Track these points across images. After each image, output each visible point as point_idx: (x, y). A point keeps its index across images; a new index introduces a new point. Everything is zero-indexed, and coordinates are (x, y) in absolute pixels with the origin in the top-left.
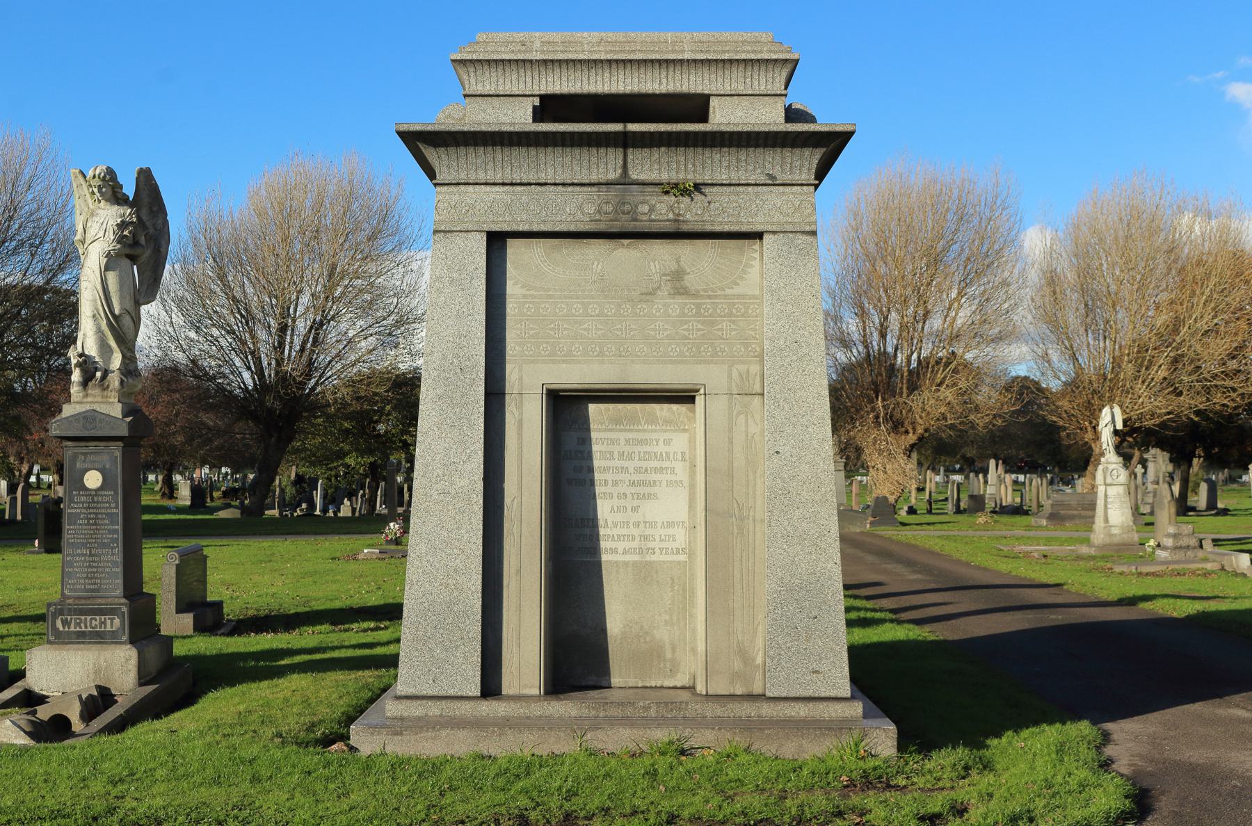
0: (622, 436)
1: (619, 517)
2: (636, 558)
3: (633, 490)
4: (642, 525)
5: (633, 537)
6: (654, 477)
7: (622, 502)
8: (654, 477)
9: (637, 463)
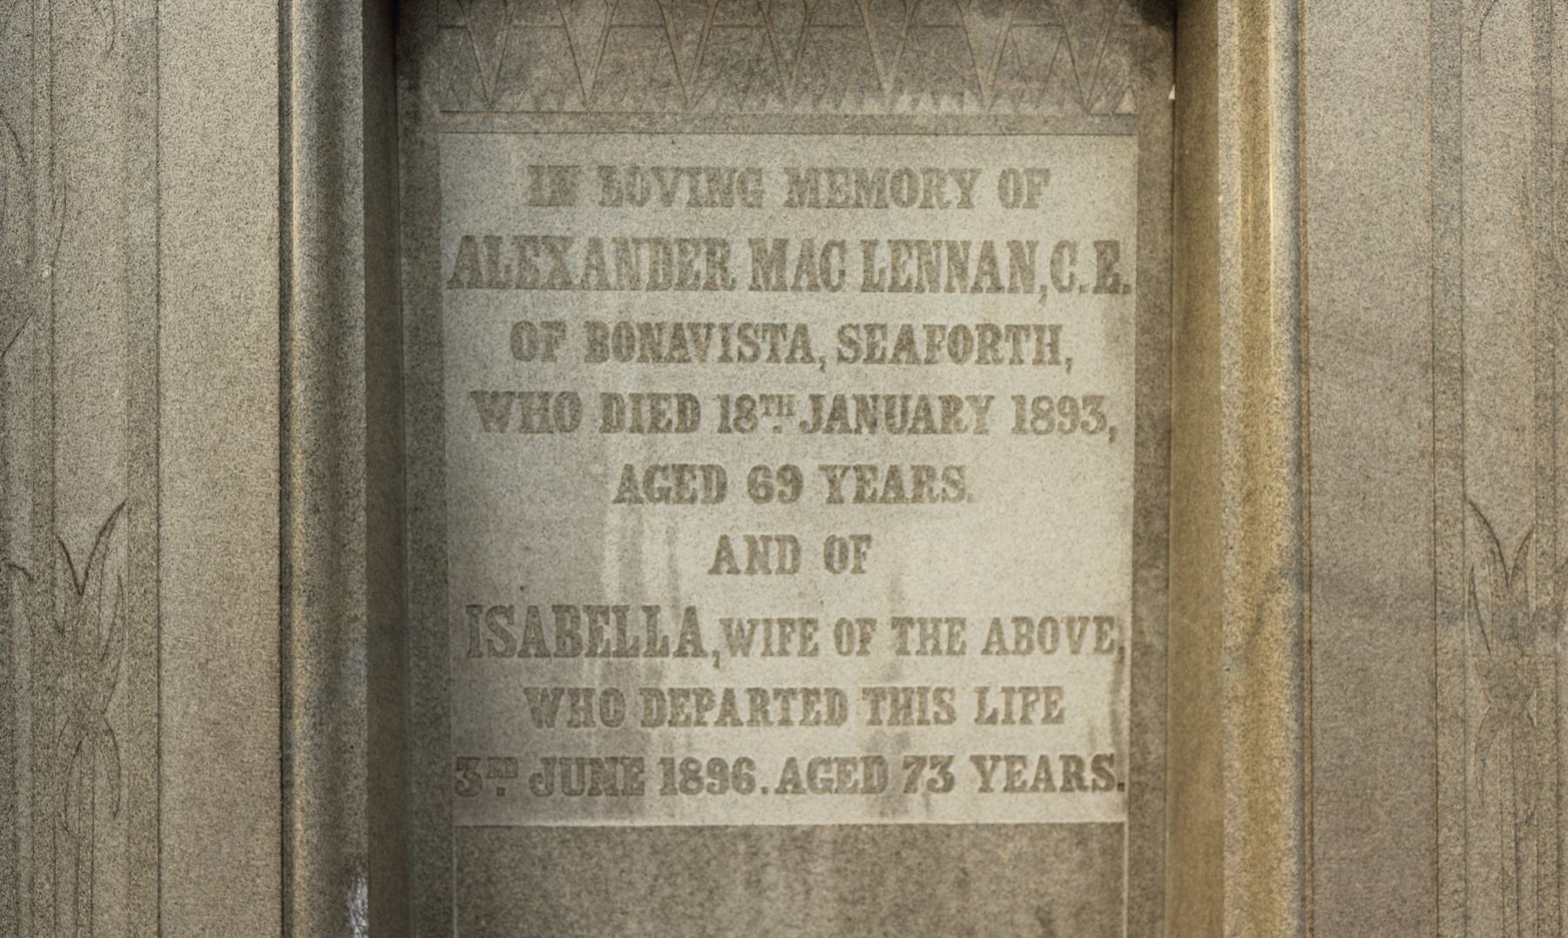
0: (776, 157)
1: (761, 597)
2: (853, 811)
3: (838, 450)
4: (884, 635)
5: (759, 490)
6: (952, 377)
7: (774, 517)
8: (952, 377)
9: (861, 308)
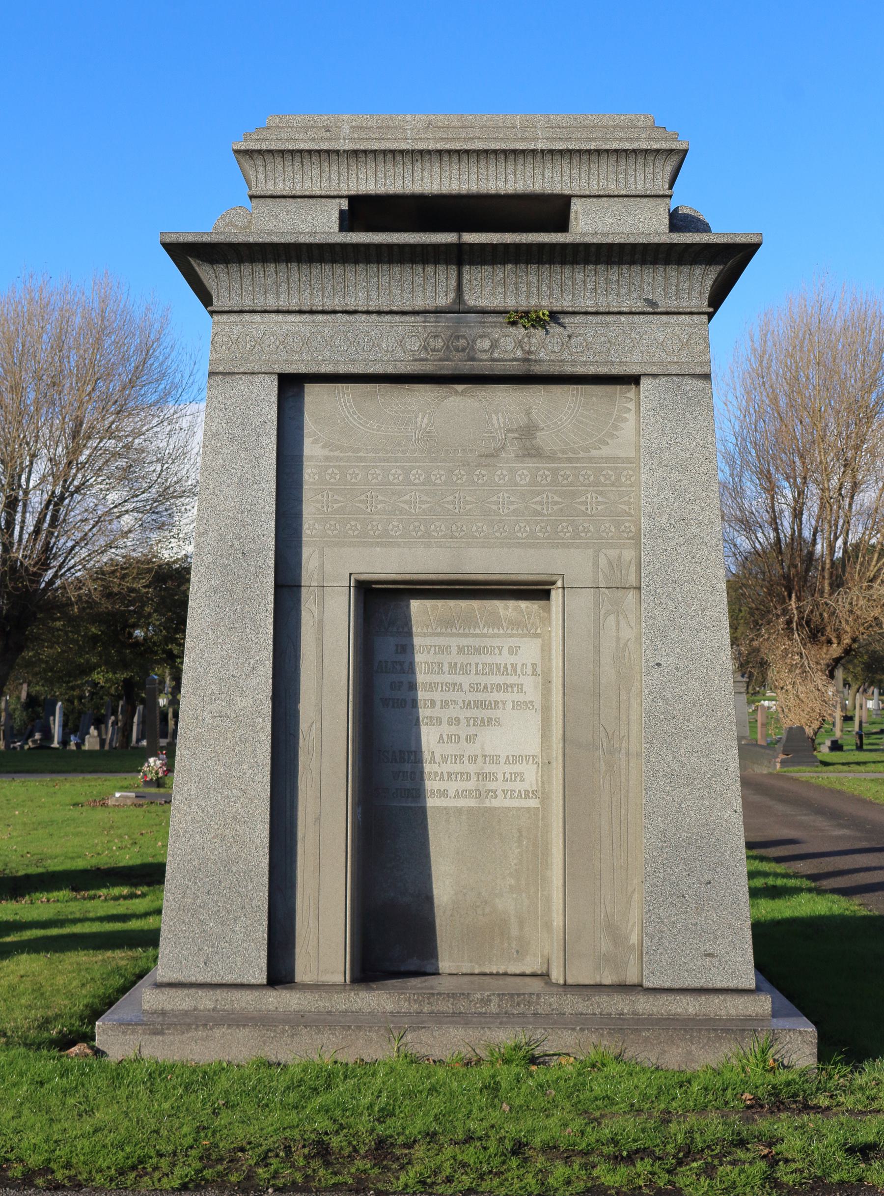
0: (454, 643)
1: (450, 749)
2: (472, 803)
3: (469, 713)
4: (480, 760)
5: (450, 723)
7: (453, 729)
9: (474, 679)
